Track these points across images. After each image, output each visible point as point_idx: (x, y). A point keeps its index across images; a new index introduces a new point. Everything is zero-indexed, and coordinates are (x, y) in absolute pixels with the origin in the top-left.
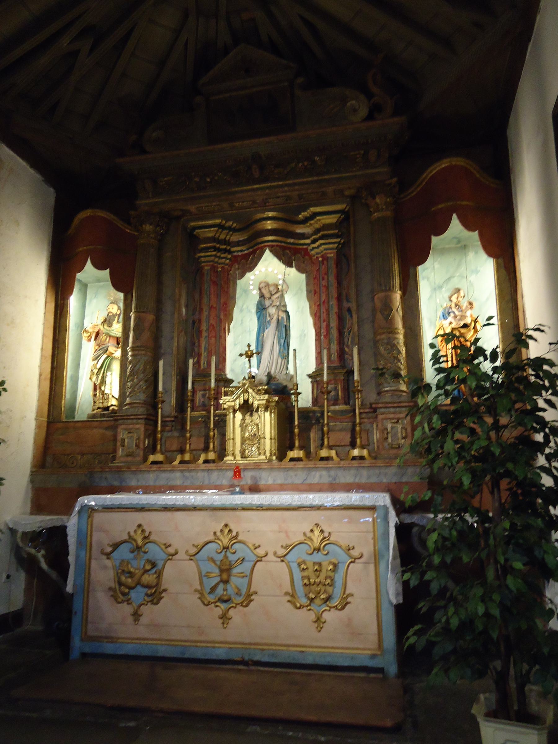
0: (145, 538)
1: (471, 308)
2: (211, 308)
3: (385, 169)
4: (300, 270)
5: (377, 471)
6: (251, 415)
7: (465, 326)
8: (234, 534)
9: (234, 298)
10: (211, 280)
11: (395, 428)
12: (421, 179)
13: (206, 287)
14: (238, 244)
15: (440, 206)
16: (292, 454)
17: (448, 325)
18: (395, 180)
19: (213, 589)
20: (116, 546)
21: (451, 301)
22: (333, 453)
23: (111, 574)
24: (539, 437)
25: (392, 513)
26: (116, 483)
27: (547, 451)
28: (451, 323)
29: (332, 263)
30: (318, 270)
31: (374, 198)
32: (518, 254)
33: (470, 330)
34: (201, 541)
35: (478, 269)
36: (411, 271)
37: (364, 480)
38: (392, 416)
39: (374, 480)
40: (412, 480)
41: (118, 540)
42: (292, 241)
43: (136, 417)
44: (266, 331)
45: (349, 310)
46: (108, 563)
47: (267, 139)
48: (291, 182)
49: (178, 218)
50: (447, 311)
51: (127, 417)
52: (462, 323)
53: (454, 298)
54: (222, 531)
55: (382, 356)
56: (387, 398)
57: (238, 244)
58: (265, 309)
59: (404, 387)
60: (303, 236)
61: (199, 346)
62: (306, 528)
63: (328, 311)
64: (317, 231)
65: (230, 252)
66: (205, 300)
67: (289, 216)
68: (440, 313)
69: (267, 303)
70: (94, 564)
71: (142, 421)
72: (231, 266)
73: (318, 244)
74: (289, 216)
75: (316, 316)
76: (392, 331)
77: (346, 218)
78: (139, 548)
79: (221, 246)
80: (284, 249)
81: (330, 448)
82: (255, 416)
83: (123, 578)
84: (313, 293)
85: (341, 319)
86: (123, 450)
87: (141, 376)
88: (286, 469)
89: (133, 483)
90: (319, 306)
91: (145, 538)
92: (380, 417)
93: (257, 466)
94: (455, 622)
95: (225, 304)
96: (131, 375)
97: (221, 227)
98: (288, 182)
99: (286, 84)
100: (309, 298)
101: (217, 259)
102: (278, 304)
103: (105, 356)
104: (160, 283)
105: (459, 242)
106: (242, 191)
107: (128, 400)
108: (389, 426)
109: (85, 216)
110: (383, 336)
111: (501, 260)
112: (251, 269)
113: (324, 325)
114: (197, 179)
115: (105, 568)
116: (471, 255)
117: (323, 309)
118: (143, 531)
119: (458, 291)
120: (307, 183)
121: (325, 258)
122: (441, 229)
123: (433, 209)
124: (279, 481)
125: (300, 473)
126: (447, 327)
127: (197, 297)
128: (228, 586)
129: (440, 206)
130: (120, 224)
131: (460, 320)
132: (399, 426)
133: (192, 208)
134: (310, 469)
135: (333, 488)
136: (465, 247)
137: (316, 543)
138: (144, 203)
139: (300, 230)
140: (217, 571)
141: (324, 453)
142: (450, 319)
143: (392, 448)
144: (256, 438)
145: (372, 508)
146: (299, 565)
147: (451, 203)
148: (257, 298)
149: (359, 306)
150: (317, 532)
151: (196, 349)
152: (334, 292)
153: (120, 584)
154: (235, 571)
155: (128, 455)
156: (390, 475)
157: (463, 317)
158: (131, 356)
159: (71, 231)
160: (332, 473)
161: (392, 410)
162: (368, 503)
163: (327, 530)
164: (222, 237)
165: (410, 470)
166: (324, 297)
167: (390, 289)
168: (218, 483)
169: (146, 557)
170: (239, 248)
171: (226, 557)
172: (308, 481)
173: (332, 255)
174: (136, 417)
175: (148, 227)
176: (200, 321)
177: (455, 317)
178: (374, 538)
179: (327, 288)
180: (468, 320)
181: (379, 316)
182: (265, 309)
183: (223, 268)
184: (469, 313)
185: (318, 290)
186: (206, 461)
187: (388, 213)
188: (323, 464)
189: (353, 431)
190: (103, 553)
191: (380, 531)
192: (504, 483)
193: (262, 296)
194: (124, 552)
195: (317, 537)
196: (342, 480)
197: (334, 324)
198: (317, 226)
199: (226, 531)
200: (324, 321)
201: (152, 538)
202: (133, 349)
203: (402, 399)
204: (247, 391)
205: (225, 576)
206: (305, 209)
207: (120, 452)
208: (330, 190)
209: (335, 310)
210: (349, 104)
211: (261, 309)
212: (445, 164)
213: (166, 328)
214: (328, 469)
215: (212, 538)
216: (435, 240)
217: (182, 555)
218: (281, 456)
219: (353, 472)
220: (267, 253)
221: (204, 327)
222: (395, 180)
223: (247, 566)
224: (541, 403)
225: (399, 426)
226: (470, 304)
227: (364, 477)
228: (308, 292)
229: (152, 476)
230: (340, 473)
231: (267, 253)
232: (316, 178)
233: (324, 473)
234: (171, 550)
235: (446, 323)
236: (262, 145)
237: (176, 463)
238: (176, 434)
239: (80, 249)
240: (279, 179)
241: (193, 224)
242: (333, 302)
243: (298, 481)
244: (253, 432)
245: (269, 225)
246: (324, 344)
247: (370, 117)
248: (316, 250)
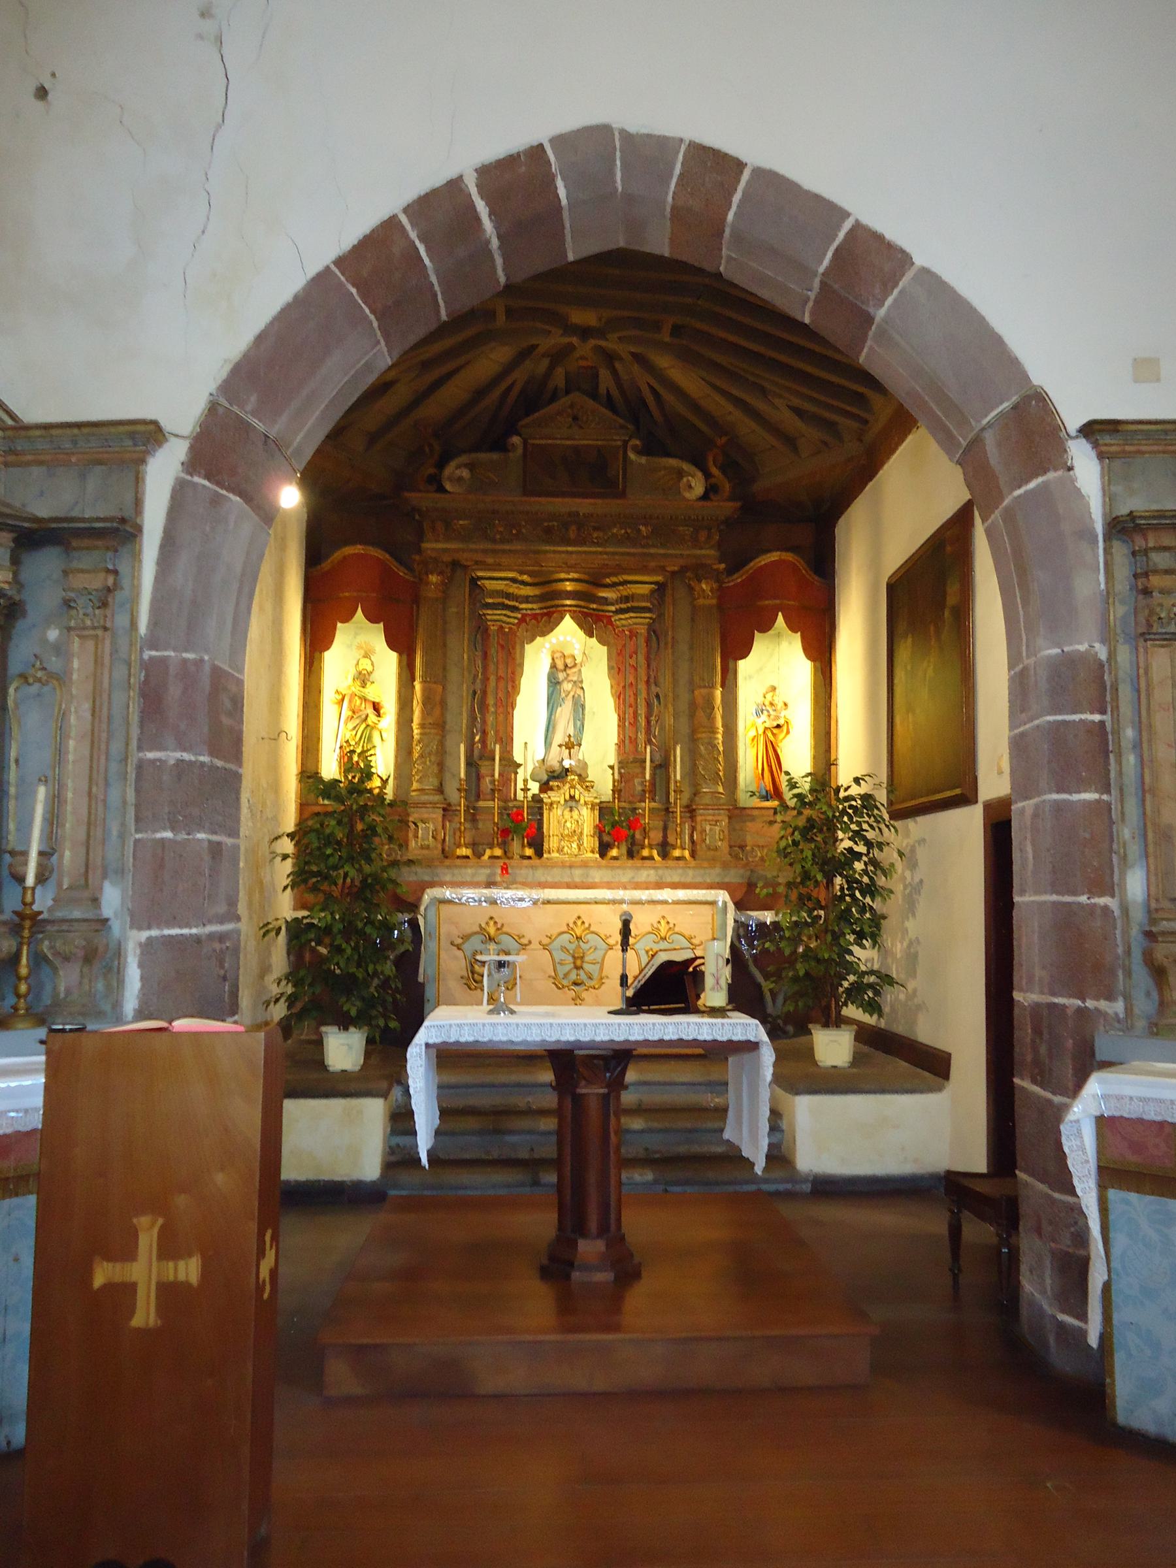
0: (498, 929)
2: (499, 679)
3: (712, 552)
4: (602, 641)
5: (702, 871)
6: (571, 811)
7: (778, 726)
8: (587, 925)
9: (522, 665)
10: (498, 643)
11: (714, 829)
12: (747, 568)
13: (493, 651)
14: (527, 599)
16: (614, 852)
18: (723, 566)
19: (566, 975)
20: (466, 938)
22: (655, 853)
23: (463, 963)
24: (861, 848)
25: (731, 906)
26: (427, 878)
27: (865, 858)
29: (642, 642)
30: (624, 646)
31: (700, 581)
34: (555, 932)
36: (731, 665)
37: (689, 880)
38: (710, 818)
39: (699, 880)
40: (733, 881)
41: (469, 931)
42: (595, 606)
43: (434, 804)
44: (559, 709)
45: (658, 696)
46: (459, 953)
47: (592, 501)
48: (612, 550)
49: (466, 567)
51: (424, 804)
53: (769, 696)
54: (575, 923)
55: (701, 756)
56: (707, 800)
57: (527, 599)
58: (559, 683)
59: (721, 790)
60: (605, 601)
61: (484, 722)
62: (654, 919)
63: (636, 695)
64: (626, 599)
65: (515, 609)
66: (492, 668)
67: (596, 580)
69: (561, 676)
70: (443, 955)
71: (441, 812)
72: (518, 625)
73: (627, 615)
74: (596, 580)
75: (620, 697)
76: (713, 731)
77: (661, 587)
78: (491, 939)
79: (507, 603)
80: (586, 615)
81: (651, 847)
82: (575, 813)
83: (477, 967)
84: (617, 668)
85: (649, 705)
86: (416, 842)
87: (433, 758)
88: (613, 868)
89: (448, 878)
90: (624, 687)
91: (498, 929)
92: (699, 818)
93: (585, 865)
94: (802, 973)
95: (513, 673)
96: (421, 756)
97: (514, 580)
98: (608, 550)
99: (619, 443)
100: (610, 676)
101: (505, 619)
102: (575, 679)
103: (364, 726)
104: (445, 645)
106: (555, 552)
107: (415, 785)
108: (708, 828)
109: (352, 552)
110: (704, 735)
111: (818, 664)
112: (544, 634)
113: (631, 710)
114: (501, 529)
115: (456, 958)
116: (784, 644)
117: (629, 692)
118: (495, 923)
119: (774, 689)
120: (628, 554)
121: (633, 634)
122: (766, 626)
124: (605, 880)
125: (628, 871)
127: (479, 662)
128: (581, 972)
130: (394, 566)
132: (717, 829)
133: (490, 560)
134: (638, 868)
135: (659, 886)
137: (663, 935)
138: (431, 546)
139: (603, 594)
140: (571, 959)
141: (645, 853)
142: (764, 717)
143: (709, 849)
144: (577, 834)
145: (713, 903)
146: (647, 952)
147: (778, 602)
148: (548, 666)
149: (676, 697)
150: (663, 922)
151: (479, 726)
152: (642, 672)
153: (473, 972)
154: (587, 959)
155: (422, 847)
156: (714, 875)
157: (777, 718)
158: (421, 734)
159: (326, 565)
160: (660, 872)
161: (711, 812)
162: (710, 899)
163: (672, 922)
164: (511, 590)
165: (733, 872)
166: (631, 679)
167: (712, 686)
168: (543, 879)
169: (500, 947)
170: (530, 606)
171: (579, 946)
172: (636, 880)
173: (643, 630)
174: (434, 804)
175: (433, 578)
176: (484, 692)
178: (713, 929)
179: (636, 669)
180: (781, 722)
181: (700, 714)
182: (559, 683)
183: (510, 629)
184: (783, 713)
185: (623, 669)
186: (491, 857)
187: (714, 601)
188: (648, 863)
189: (665, 829)
190: (452, 944)
191: (718, 922)
192: (838, 880)
193: (554, 666)
194: (475, 943)
195: (663, 928)
196: (669, 880)
197: (642, 711)
198: (625, 593)
199: (579, 923)
200: (631, 706)
201: (504, 929)
202: (422, 726)
203: (722, 801)
204: (574, 788)
205: (579, 963)
206: (615, 575)
207: (413, 844)
208: (653, 564)
209: (643, 694)
210: (685, 479)
211: (554, 683)
212: (774, 556)
213: (452, 701)
214: (654, 868)
215: (565, 929)
217: (535, 945)
218: (603, 854)
219: (680, 871)
220: (568, 618)
221: (491, 701)
222: (723, 566)
223: (600, 953)
224: (865, 826)
225: (717, 829)
226: (786, 705)
227: (690, 876)
228: (610, 668)
229: (469, 871)
230: (667, 872)
231: (568, 618)
232: (640, 550)
233: (652, 872)
234: (524, 941)
235: (759, 721)
236: (584, 506)
237: (486, 857)
238: (468, 825)
239: (347, 594)
240: (598, 544)
241: (480, 574)
242: (642, 687)
243: (625, 879)
244: (571, 825)
245: (569, 586)
246: (629, 732)
247: (705, 497)
248: (624, 622)
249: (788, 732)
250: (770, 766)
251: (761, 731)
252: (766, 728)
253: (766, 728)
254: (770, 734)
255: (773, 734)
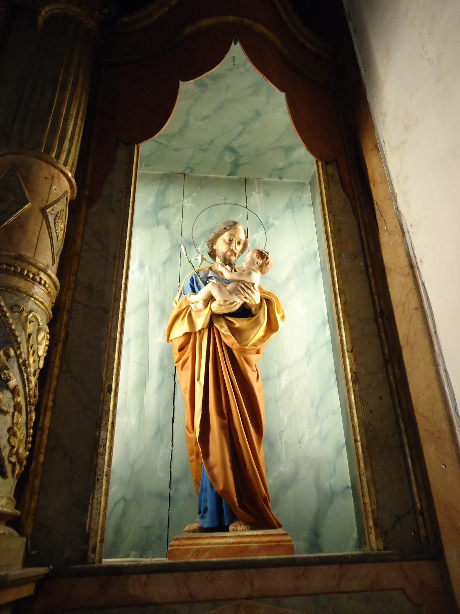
1: (263, 268)
7: (245, 312)
15: (205, 23)
17: (200, 305)
21: (213, 254)
28: (210, 299)
32: (377, 147)
33: (257, 323)
35: (271, 221)
36: (121, 154)
50: (202, 274)
52: (239, 302)
53: (221, 247)
68: (186, 283)
105: (236, 165)
123: (188, 30)
126: (199, 311)
129: (205, 23)
131: (235, 292)
136: (246, 182)
142: (210, 288)
147: (231, 19)
157: (243, 286)
177: (223, 282)
216: (184, 86)
249: (272, 327)
250: (225, 414)
251: (201, 321)
252: (214, 317)
253: (214, 317)
254: (224, 330)
255: (235, 332)
